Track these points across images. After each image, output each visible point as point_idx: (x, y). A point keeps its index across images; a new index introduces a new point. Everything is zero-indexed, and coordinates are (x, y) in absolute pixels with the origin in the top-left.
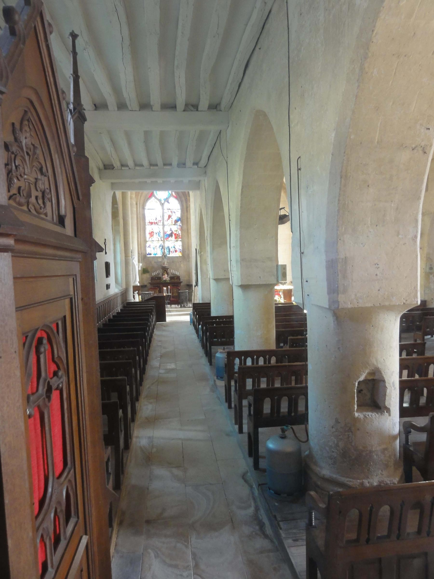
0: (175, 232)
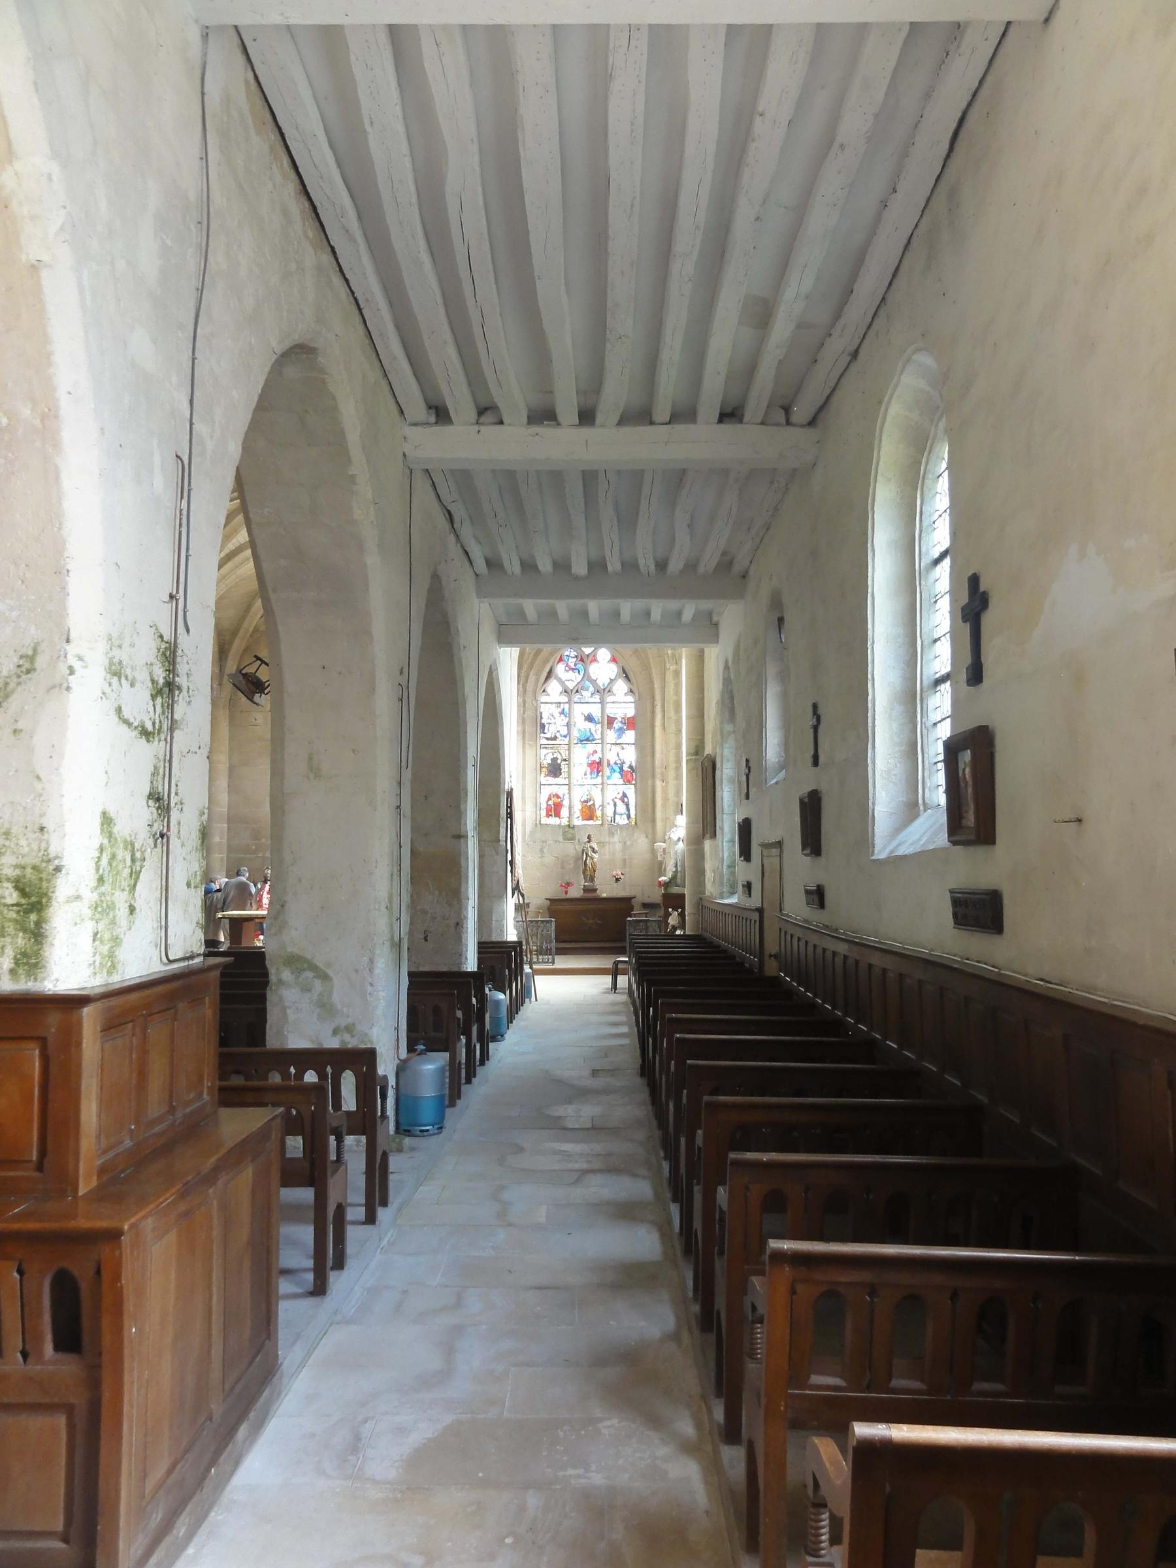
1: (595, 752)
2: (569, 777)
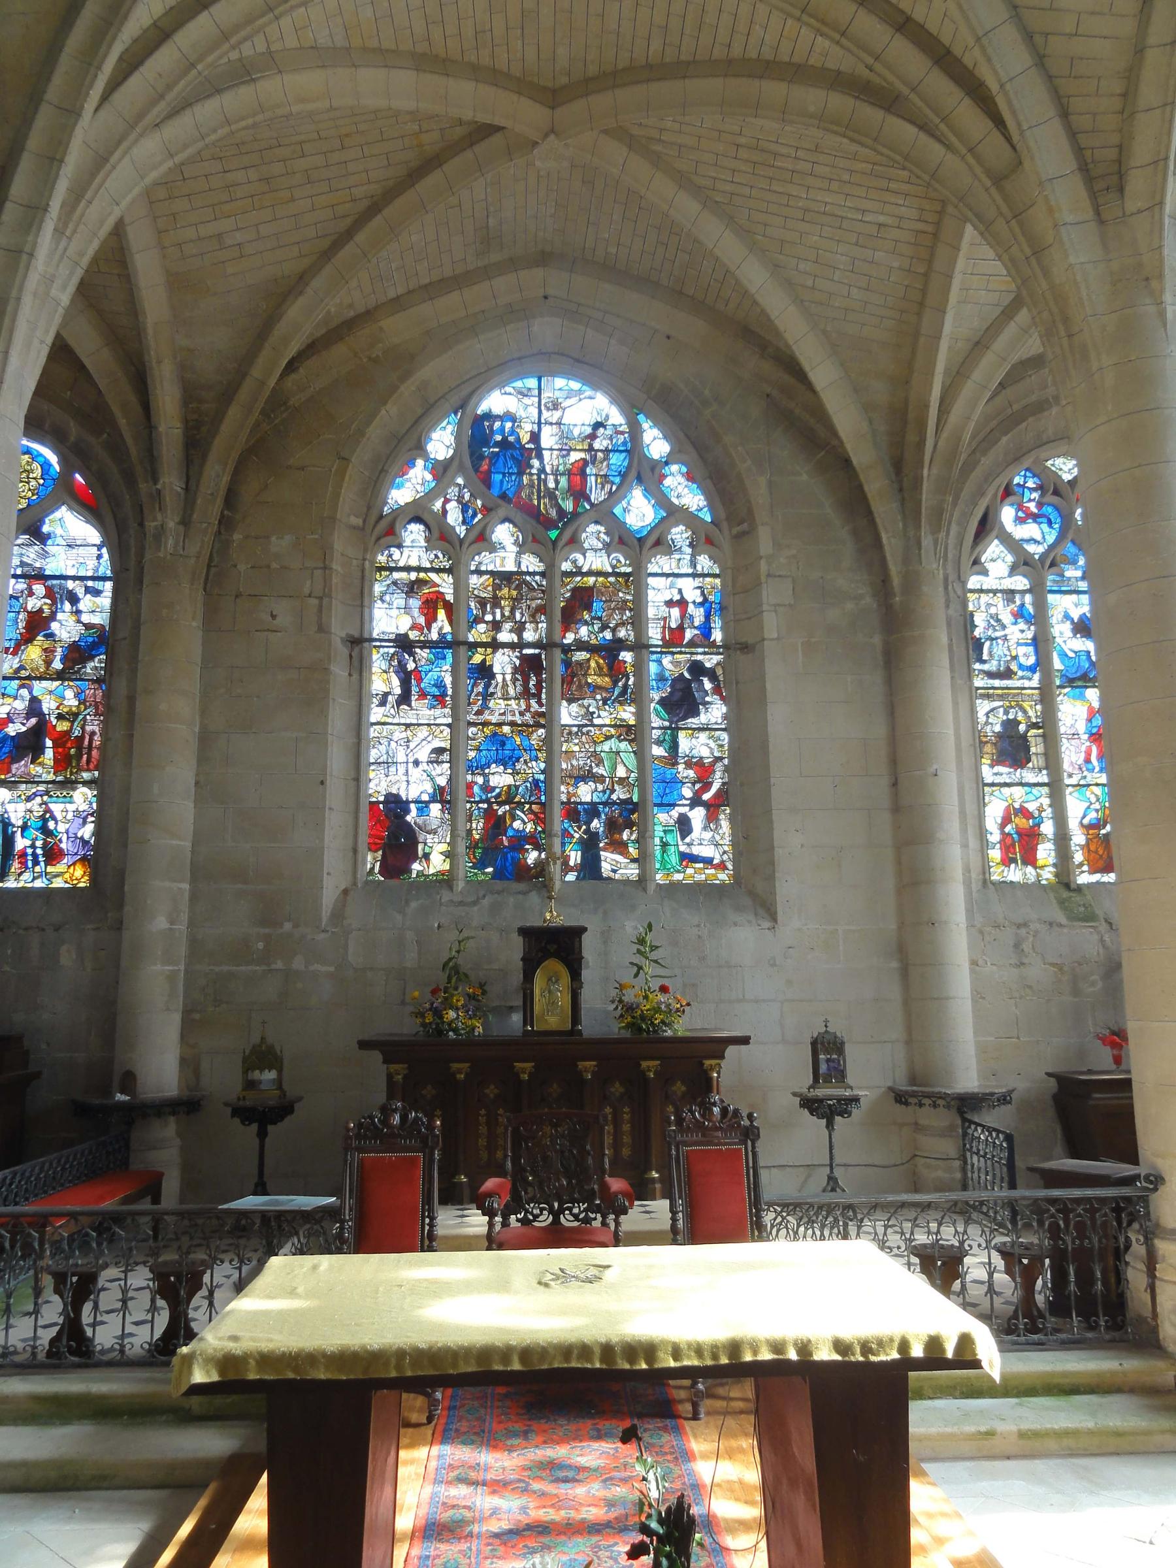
0: (63, 726)
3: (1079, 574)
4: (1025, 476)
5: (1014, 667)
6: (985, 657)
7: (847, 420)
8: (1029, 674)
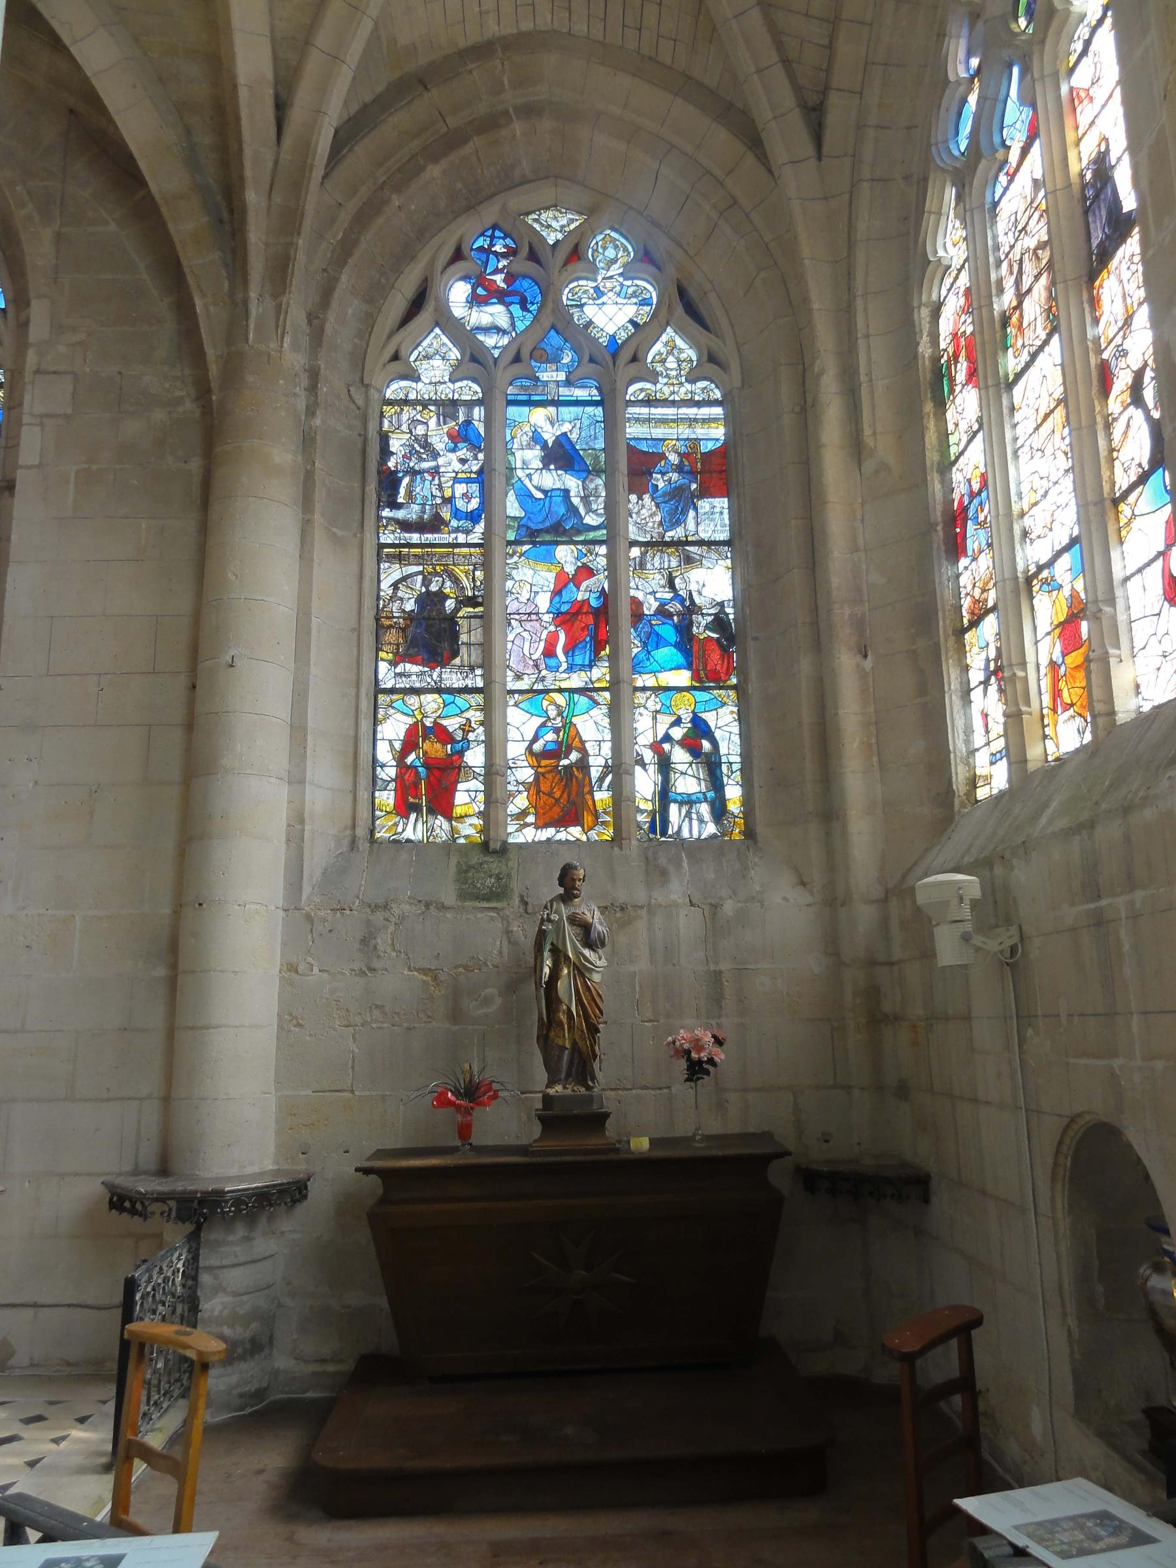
1: (586, 572)
2: (486, 664)
3: (562, 376)
4: (492, 237)
5: (446, 514)
6: (400, 500)
7: (138, 123)
8: (469, 524)
